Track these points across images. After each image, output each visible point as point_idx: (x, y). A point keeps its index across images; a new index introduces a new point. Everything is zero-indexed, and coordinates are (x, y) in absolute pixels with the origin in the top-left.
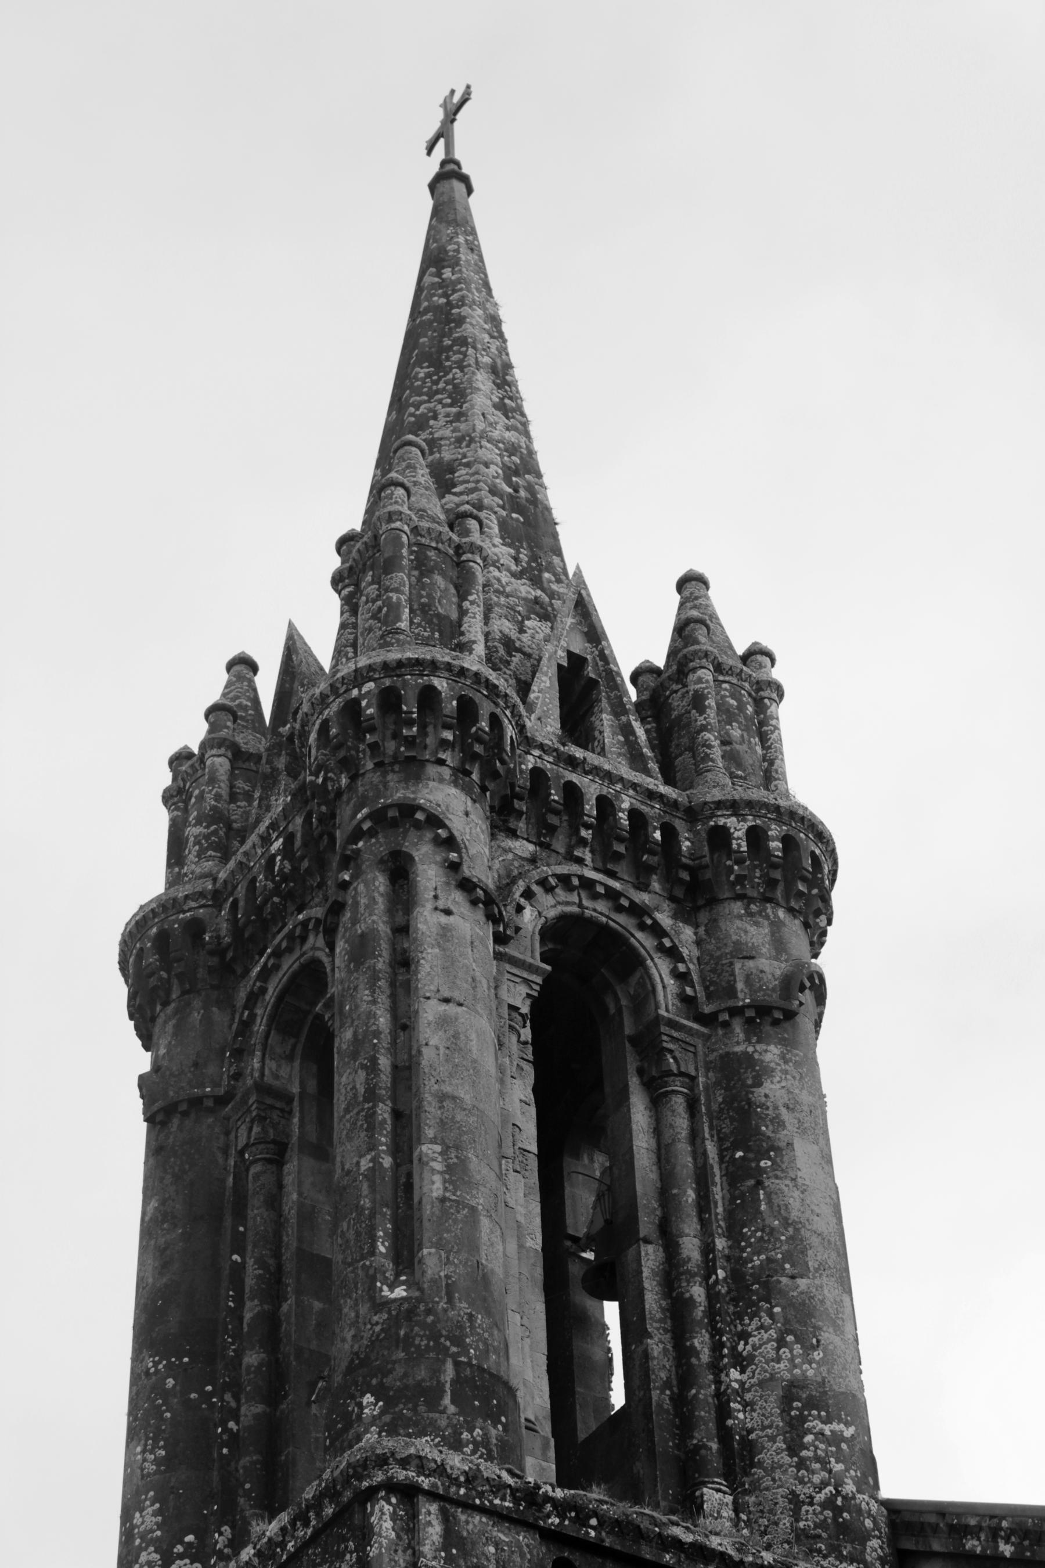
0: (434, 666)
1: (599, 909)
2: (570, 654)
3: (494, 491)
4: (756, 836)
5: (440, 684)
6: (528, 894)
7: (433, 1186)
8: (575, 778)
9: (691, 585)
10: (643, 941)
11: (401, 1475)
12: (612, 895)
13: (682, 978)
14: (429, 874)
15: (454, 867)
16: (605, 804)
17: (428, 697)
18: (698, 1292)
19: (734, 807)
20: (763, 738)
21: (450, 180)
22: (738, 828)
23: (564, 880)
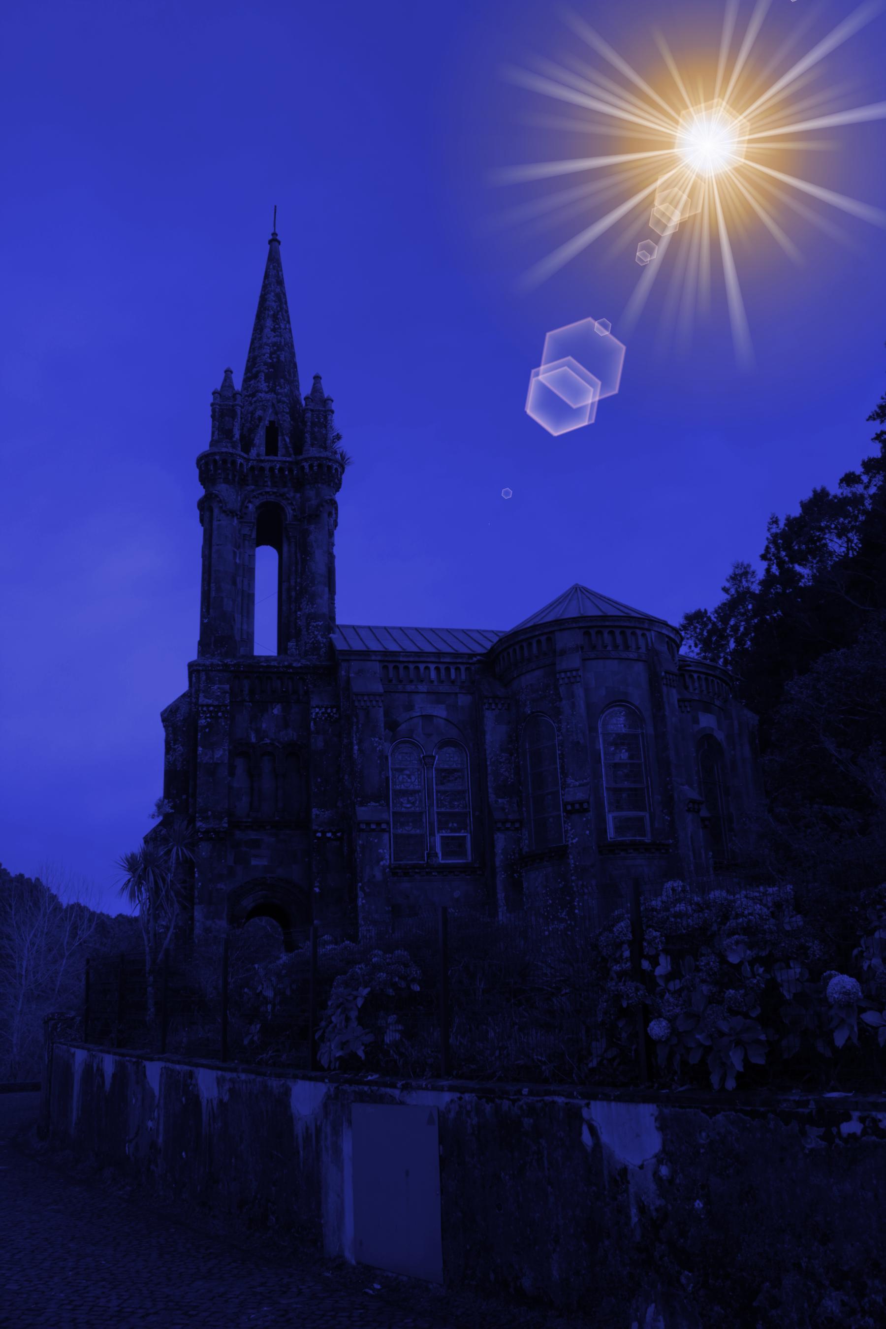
0: (215, 454)
2: (270, 422)
3: (265, 364)
4: (311, 466)
5: (217, 457)
6: (250, 502)
7: (213, 594)
8: (263, 465)
9: (317, 378)
11: (195, 668)
12: (274, 493)
13: (294, 510)
14: (216, 511)
15: (221, 507)
16: (272, 469)
17: (215, 461)
18: (293, 594)
19: (306, 460)
20: (326, 427)
21: (274, 241)
22: (306, 465)
23: (261, 494)
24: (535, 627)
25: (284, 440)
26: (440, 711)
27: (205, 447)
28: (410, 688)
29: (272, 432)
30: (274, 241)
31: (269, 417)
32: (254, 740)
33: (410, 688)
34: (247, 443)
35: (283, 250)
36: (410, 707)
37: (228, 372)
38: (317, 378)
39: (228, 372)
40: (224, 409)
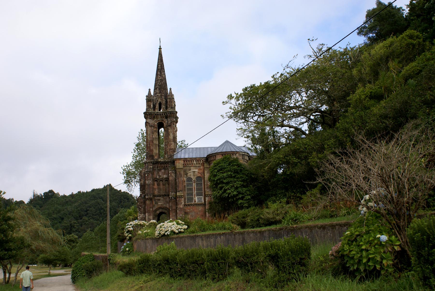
1: (161, 121)
9: (170, 89)
10: (163, 122)
21: (160, 49)
24: (212, 154)
25: (163, 106)
26: (197, 170)
27: (145, 111)
28: (190, 166)
29: (160, 105)
30: (160, 49)
31: (159, 100)
32: (158, 177)
33: (190, 166)
34: (154, 108)
35: (162, 50)
36: (190, 170)
37: (150, 90)
38: (170, 89)
39: (150, 90)
40: (149, 99)
